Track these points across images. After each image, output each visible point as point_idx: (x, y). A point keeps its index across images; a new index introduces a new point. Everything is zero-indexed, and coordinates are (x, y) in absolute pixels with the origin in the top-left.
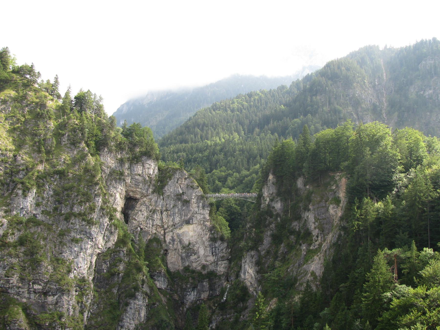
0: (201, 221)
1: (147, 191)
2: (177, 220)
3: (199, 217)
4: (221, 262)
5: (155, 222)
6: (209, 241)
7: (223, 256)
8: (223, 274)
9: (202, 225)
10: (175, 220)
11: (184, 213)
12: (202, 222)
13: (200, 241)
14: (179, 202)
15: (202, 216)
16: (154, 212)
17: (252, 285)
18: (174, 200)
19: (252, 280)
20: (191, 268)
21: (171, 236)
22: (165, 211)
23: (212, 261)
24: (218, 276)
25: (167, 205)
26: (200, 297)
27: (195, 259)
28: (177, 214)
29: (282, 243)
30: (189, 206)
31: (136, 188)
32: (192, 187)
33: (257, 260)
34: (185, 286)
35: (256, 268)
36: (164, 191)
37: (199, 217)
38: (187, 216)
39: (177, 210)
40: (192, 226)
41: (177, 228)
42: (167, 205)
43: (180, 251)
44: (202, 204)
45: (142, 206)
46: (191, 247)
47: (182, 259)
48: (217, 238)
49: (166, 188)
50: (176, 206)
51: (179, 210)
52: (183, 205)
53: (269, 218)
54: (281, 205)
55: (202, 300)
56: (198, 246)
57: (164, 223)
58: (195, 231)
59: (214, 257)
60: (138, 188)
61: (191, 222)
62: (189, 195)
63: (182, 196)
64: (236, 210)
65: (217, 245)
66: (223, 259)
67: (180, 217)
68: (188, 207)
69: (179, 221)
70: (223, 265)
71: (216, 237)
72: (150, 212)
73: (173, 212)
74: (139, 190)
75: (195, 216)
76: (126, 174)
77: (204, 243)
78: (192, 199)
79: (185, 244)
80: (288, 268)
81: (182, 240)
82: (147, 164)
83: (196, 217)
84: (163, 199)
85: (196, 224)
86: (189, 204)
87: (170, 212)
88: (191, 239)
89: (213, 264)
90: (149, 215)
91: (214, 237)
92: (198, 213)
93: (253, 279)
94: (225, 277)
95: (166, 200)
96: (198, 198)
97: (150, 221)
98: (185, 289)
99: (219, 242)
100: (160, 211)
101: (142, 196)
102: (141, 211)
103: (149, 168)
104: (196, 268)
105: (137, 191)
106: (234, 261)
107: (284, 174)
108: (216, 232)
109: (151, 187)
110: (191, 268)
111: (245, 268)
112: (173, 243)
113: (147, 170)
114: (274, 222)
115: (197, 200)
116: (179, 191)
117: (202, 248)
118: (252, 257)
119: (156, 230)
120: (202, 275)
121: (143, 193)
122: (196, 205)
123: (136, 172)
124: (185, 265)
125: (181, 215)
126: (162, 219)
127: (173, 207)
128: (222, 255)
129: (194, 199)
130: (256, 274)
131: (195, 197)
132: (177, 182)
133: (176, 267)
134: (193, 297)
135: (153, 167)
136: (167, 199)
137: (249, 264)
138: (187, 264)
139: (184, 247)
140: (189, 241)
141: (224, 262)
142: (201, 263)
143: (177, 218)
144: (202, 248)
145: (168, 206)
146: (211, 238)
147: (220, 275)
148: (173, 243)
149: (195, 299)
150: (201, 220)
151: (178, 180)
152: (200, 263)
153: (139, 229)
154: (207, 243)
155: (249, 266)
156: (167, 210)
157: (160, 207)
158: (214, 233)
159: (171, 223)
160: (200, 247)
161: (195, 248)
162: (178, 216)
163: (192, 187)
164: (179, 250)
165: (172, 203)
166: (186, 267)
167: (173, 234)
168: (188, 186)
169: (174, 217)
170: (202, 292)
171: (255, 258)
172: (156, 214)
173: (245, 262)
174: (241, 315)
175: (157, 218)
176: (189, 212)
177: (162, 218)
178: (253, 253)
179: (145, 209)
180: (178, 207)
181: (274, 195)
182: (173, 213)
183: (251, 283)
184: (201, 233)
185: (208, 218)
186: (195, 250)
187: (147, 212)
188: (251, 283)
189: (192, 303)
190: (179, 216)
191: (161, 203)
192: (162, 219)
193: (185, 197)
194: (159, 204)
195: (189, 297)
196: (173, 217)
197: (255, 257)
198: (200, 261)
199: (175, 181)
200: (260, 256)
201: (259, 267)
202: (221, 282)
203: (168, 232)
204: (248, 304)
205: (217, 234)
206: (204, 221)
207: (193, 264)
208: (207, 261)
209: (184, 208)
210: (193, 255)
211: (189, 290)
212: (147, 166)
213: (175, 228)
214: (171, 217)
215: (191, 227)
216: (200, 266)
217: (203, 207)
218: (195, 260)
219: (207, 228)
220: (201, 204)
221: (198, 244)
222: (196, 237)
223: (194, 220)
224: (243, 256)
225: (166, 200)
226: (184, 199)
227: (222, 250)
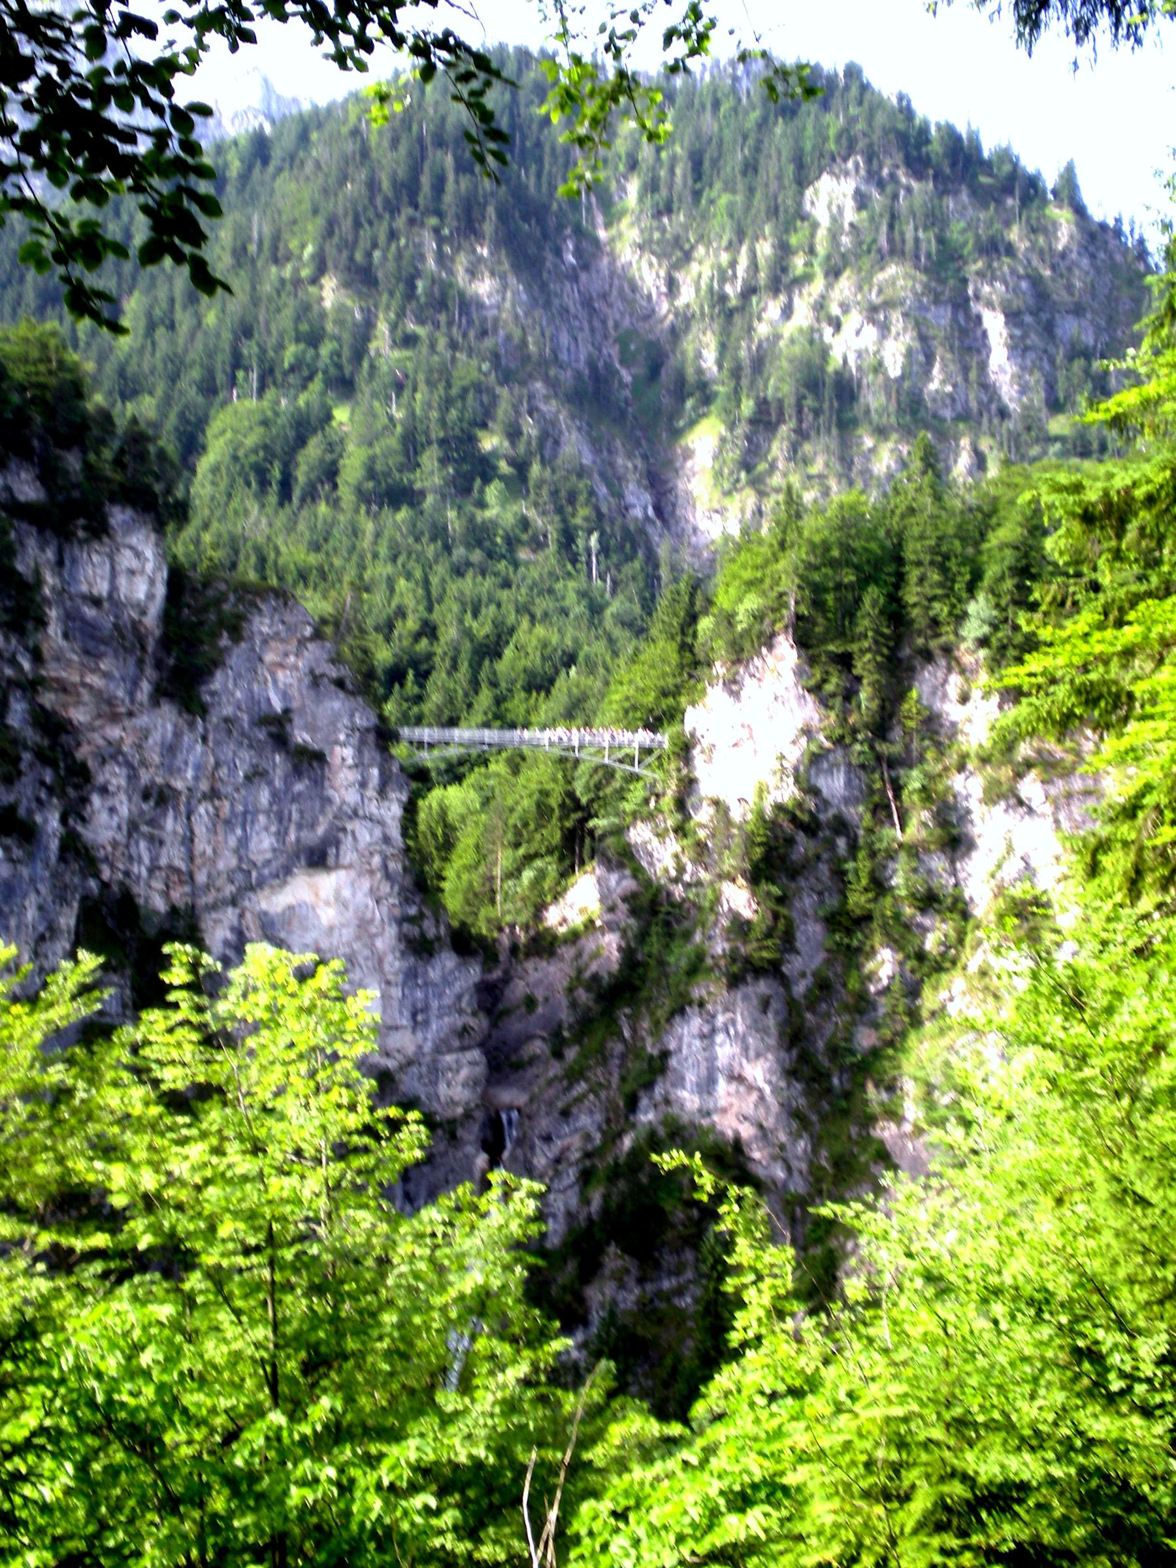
1: (131, 694)
2: (263, 844)
3: (365, 835)
5: (164, 851)
6: (403, 953)
7: (465, 1031)
8: (468, 1115)
10: (252, 845)
11: (301, 812)
12: (376, 860)
13: (367, 952)
15: (378, 832)
16: (161, 797)
18: (251, 746)
19: (762, 1111)
21: (233, 929)
22: (206, 797)
28: (262, 819)
30: (323, 777)
31: (84, 668)
32: (340, 684)
36: (207, 698)
37: (365, 835)
38: (313, 826)
39: (264, 797)
41: (261, 884)
42: (217, 765)
44: (382, 774)
45: (108, 768)
48: (438, 938)
49: (218, 682)
51: (275, 795)
52: (297, 773)
54: (848, 783)
57: (198, 861)
58: (345, 905)
59: (420, 1035)
60: (96, 670)
61: (331, 860)
62: (322, 722)
65: (434, 974)
66: (466, 1042)
67: (278, 834)
68: (319, 783)
70: (464, 1073)
72: (146, 796)
73: (246, 805)
74: (94, 680)
75: (349, 827)
76: (47, 591)
77: (380, 961)
78: (337, 742)
82: (128, 553)
84: (204, 739)
85: (350, 867)
87: (227, 804)
89: (414, 1069)
90: (142, 813)
91: (423, 935)
93: (767, 1108)
95: (218, 743)
96: (363, 742)
97: (143, 845)
99: (447, 960)
100: (184, 798)
101: (99, 716)
102: (104, 791)
103: (132, 572)
105: (84, 684)
109: (149, 671)
111: (711, 1059)
113: (122, 582)
115: (359, 751)
116: (268, 700)
118: (765, 1004)
119: (166, 894)
121: (110, 702)
123: (84, 588)
126: (189, 840)
127: (248, 778)
129: (344, 745)
130: (783, 1084)
135: (149, 567)
136: (222, 735)
143: (264, 834)
145: (223, 772)
153: (93, 884)
154: (394, 964)
156: (213, 794)
157: (190, 774)
158: (421, 916)
159: (227, 862)
165: (244, 760)
167: (241, 916)
168: (316, 680)
171: (776, 1013)
172: (171, 813)
175: (175, 832)
176: (322, 811)
177: (192, 832)
178: (763, 987)
179: (123, 782)
180: (270, 783)
182: (245, 813)
183: (761, 1127)
184: (369, 915)
187: (130, 800)
188: (761, 1127)
190: (273, 829)
191: (195, 752)
192: (192, 840)
193: (301, 736)
194: (186, 763)
196: (239, 832)
197: (775, 1005)
199: (253, 650)
200: (791, 1005)
203: (214, 907)
209: (299, 787)
212: (126, 559)
213: (252, 889)
214: (233, 831)
215: (328, 883)
217: (382, 792)
220: (375, 772)
222: (348, 933)
223: (343, 848)
225: (218, 743)
226: (298, 746)
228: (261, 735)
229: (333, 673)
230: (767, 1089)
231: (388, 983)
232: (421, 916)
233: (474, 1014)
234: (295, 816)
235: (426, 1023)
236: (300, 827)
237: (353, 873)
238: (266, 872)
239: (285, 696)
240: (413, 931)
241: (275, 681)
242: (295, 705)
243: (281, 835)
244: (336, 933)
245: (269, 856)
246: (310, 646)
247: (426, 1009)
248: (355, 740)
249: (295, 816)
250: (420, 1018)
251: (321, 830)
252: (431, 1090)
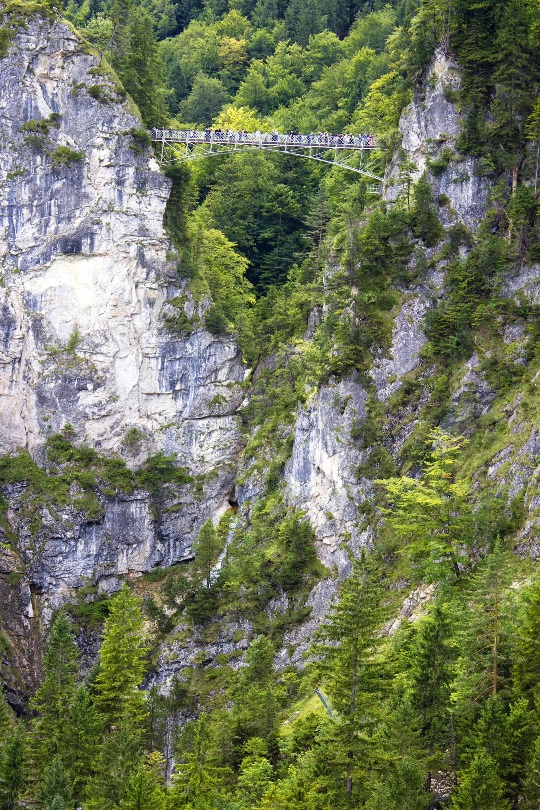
0: (129, 245)
4: (206, 421)
7: (217, 400)
8: (214, 474)
9: (130, 259)
11: (59, 206)
12: (133, 250)
14: (38, 159)
15: (135, 224)
17: (333, 525)
19: (333, 503)
20: (78, 443)
23: (170, 415)
24: (190, 481)
26: (113, 564)
27: (95, 405)
28: (25, 211)
29: (469, 357)
30: (80, 177)
32: (95, 93)
33: (360, 422)
34: (50, 518)
35: (354, 452)
39: (25, 194)
40: (92, 260)
41: (24, 270)
43: (36, 367)
46: (81, 355)
47: (42, 400)
50: (21, 175)
52: (55, 173)
53: (420, 245)
55: (121, 577)
56: (110, 348)
59: (180, 402)
61: (85, 249)
63: (52, 130)
64: (282, 204)
65: (192, 349)
69: (36, 239)
71: (190, 314)
79: (58, 341)
80: (487, 464)
81: (44, 323)
83: (108, 224)
85: (106, 254)
86: (80, 168)
88: (83, 321)
89: (173, 429)
92: (117, 208)
94: (223, 487)
98: (50, 528)
104: (98, 444)
106: (262, 422)
107: (500, 56)
108: (190, 296)
110: (78, 443)
111: (306, 451)
112: (7, 335)
114: (442, 264)
116: (36, 108)
117: (127, 360)
120: (127, 475)
122: (110, 174)
124: (54, 429)
128: (213, 393)
129: (100, 147)
130: (353, 480)
131: (106, 139)
132: (30, 71)
133: (13, 435)
134: (82, 563)
137: (323, 438)
138: (62, 427)
139: (53, 355)
140: (76, 327)
141: (220, 422)
142: (123, 423)
143: (28, 225)
144: (132, 358)
146: (169, 321)
147: (201, 478)
148: (7, 335)
149: (90, 572)
150: (128, 239)
151: (34, 58)
152: (117, 423)
155: (326, 445)
160: (122, 354)
161: (100, 358)
162: (29, 220)
163: (95, 93)
164: (28, 363)
166: (59, 438)
167: (8, 294)
169: (11, 221)
170: (121, 546)
171: (353, 412)
173: (311, 425)
174: (279, 647)
176: (77, 206)
180: (31, 181)
181: (450, 146)
182: (10, 207)
183: (330, 517)
184: (126, 297)
185: (160, 236)
186: (99, 366)
188: (330, 517)
189: (77, 588)
190: (36, 221)
195: (68, 563)
198: (118, 416)
201: (369, 451)
202: (204, 506)
204: (311, 603)
205: (197, 303)
206: (143, 246)
207: (88, 425)
208: (148, 417)
209: (58, 185)
210: (90, 386)
211: (69, 534)
213: (17, 272)
216: (116, 435)
218: (95, 410)
219: (153, 274)
220: (131, 171)
221: (111, 343)
222: (108, 311)
223: (97, 238)
224: (303, 401)
226: (60, 147)
227: (216, 371)
228: (20, 139)
229: (91, 83)
230: (340, 483)
231: (146, 356)
232: (184, 299)
233: (229, 386)
234: (54, 209)
235: (186, 392)
236: (59, 220)
237: (108, 260)
239: (54, 105)
240: (171, 311)
241: (45, 92)
242: (61, 112)
244: (94, 311)
245: (32, 244)
246: (75, 59)
247: (184, 378)
248: (113, 144)
249: (54, 209)
250: (178, 387)
251: (77, 223)
252: (185, 448)
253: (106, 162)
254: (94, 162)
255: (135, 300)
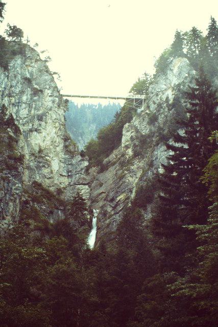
11: (36, 105)
25: (11, 87)
28: (24, 106)
38: (38, 110)
42: (11, 87)
75: (50, 112)
116: (26, 74)
125: (30, 106)
154: (62, 155)
169: (18, 108)
182: (19, 102)
196: (17, 108)
234: (34, 106)
236: (35, 109)
238: (25, 120)
243: (29, 111)
245: (26, 116)
253: (50, 94)
254: (46, 94)
255: (57, 141)
